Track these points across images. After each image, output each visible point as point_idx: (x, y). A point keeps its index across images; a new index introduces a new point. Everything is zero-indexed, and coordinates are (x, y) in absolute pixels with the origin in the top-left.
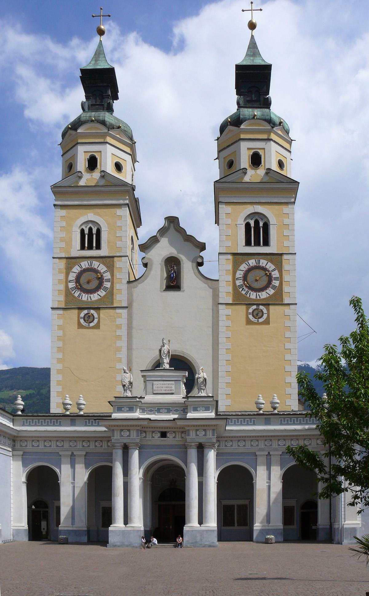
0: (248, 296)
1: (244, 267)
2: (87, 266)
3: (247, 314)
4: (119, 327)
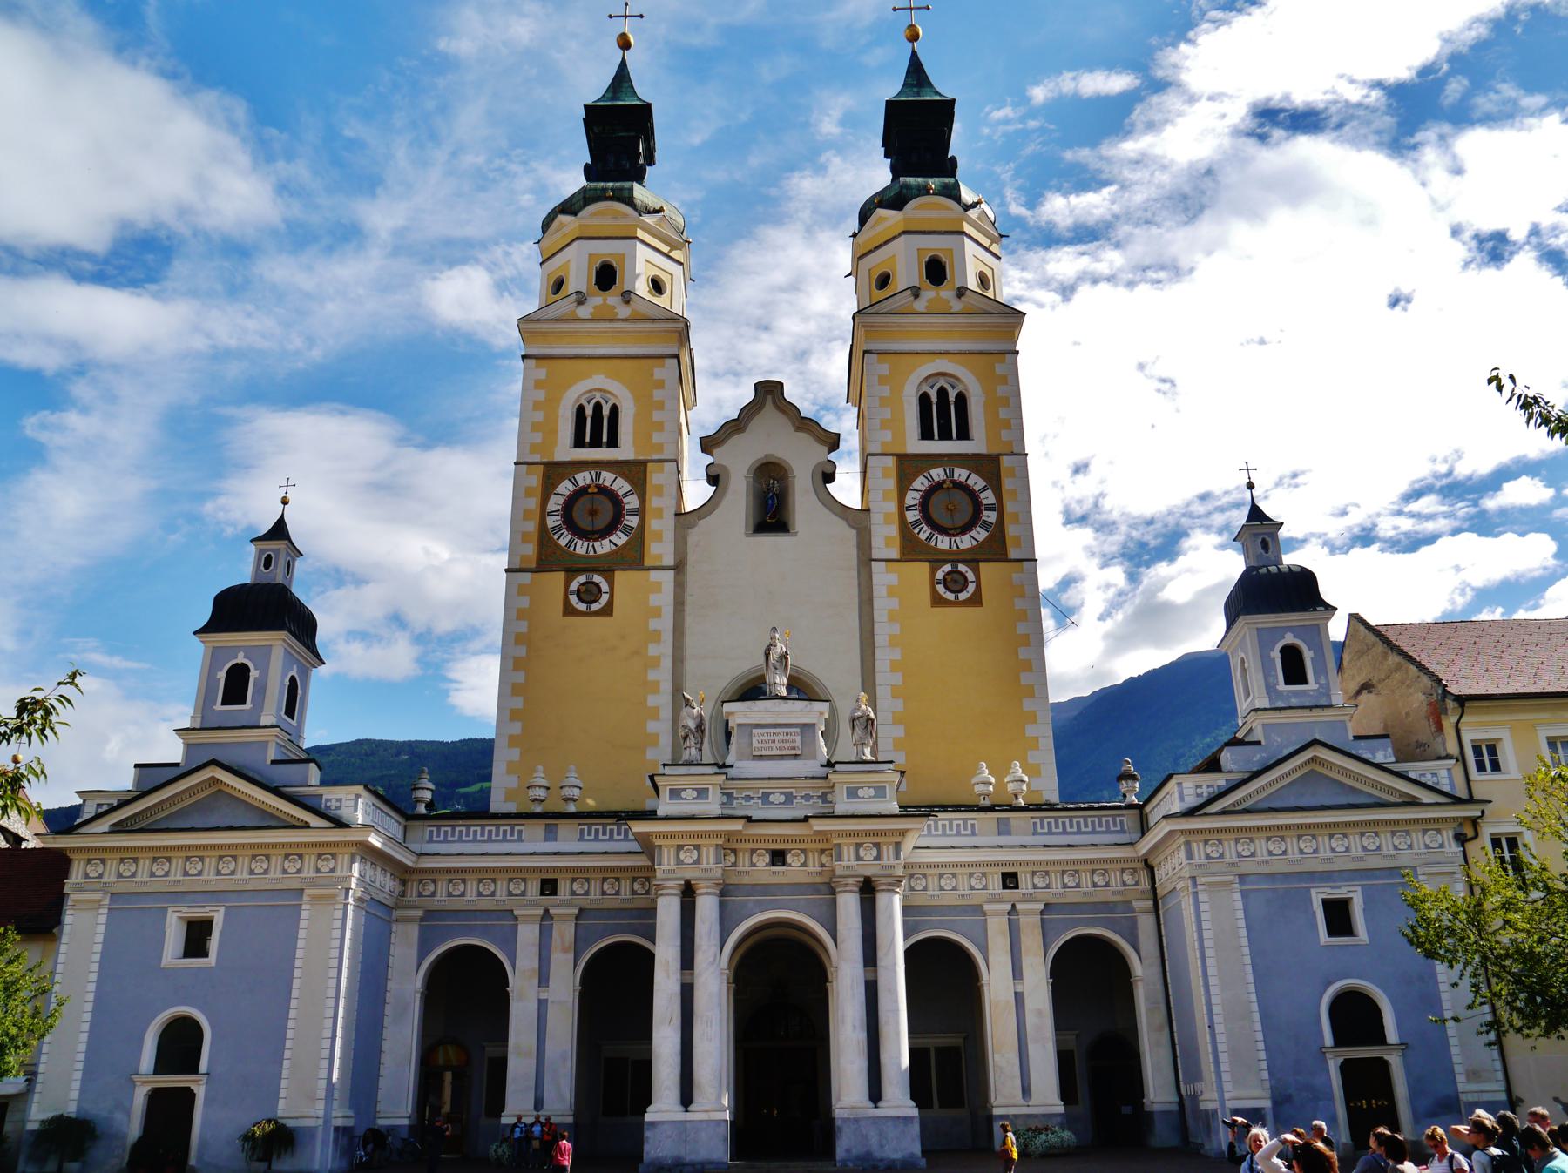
1: (921, 483)
3: (933, 582)
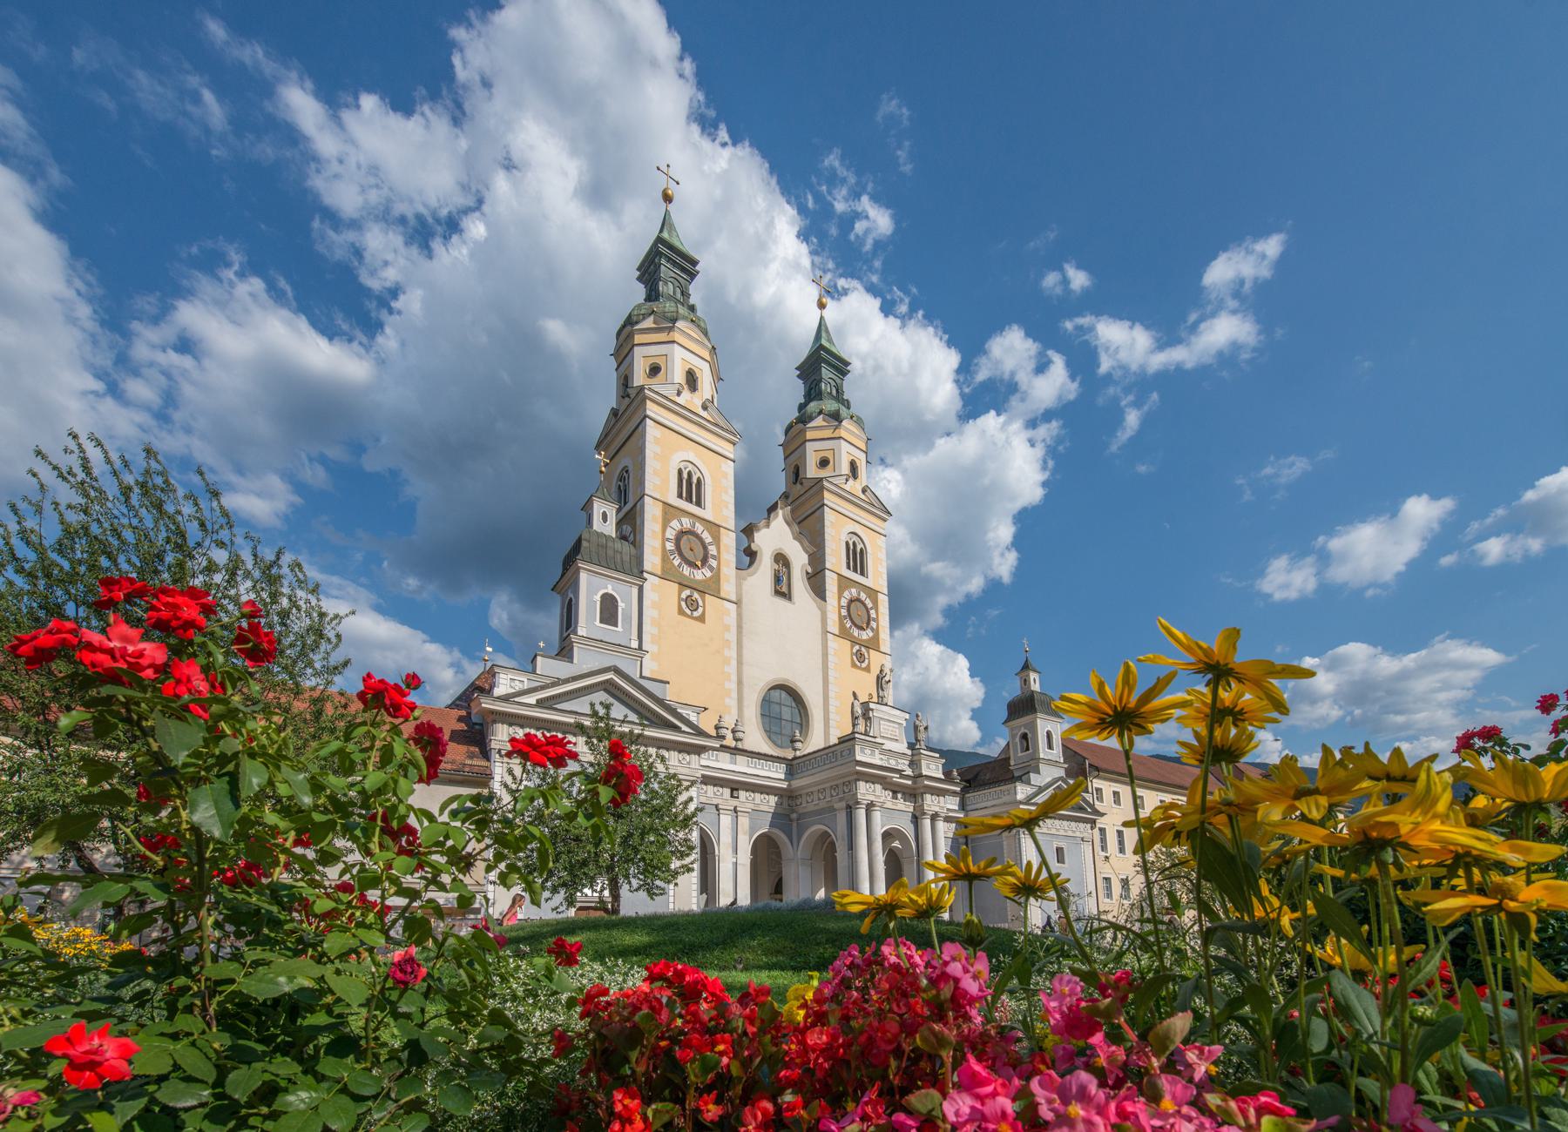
4: (727, 628)
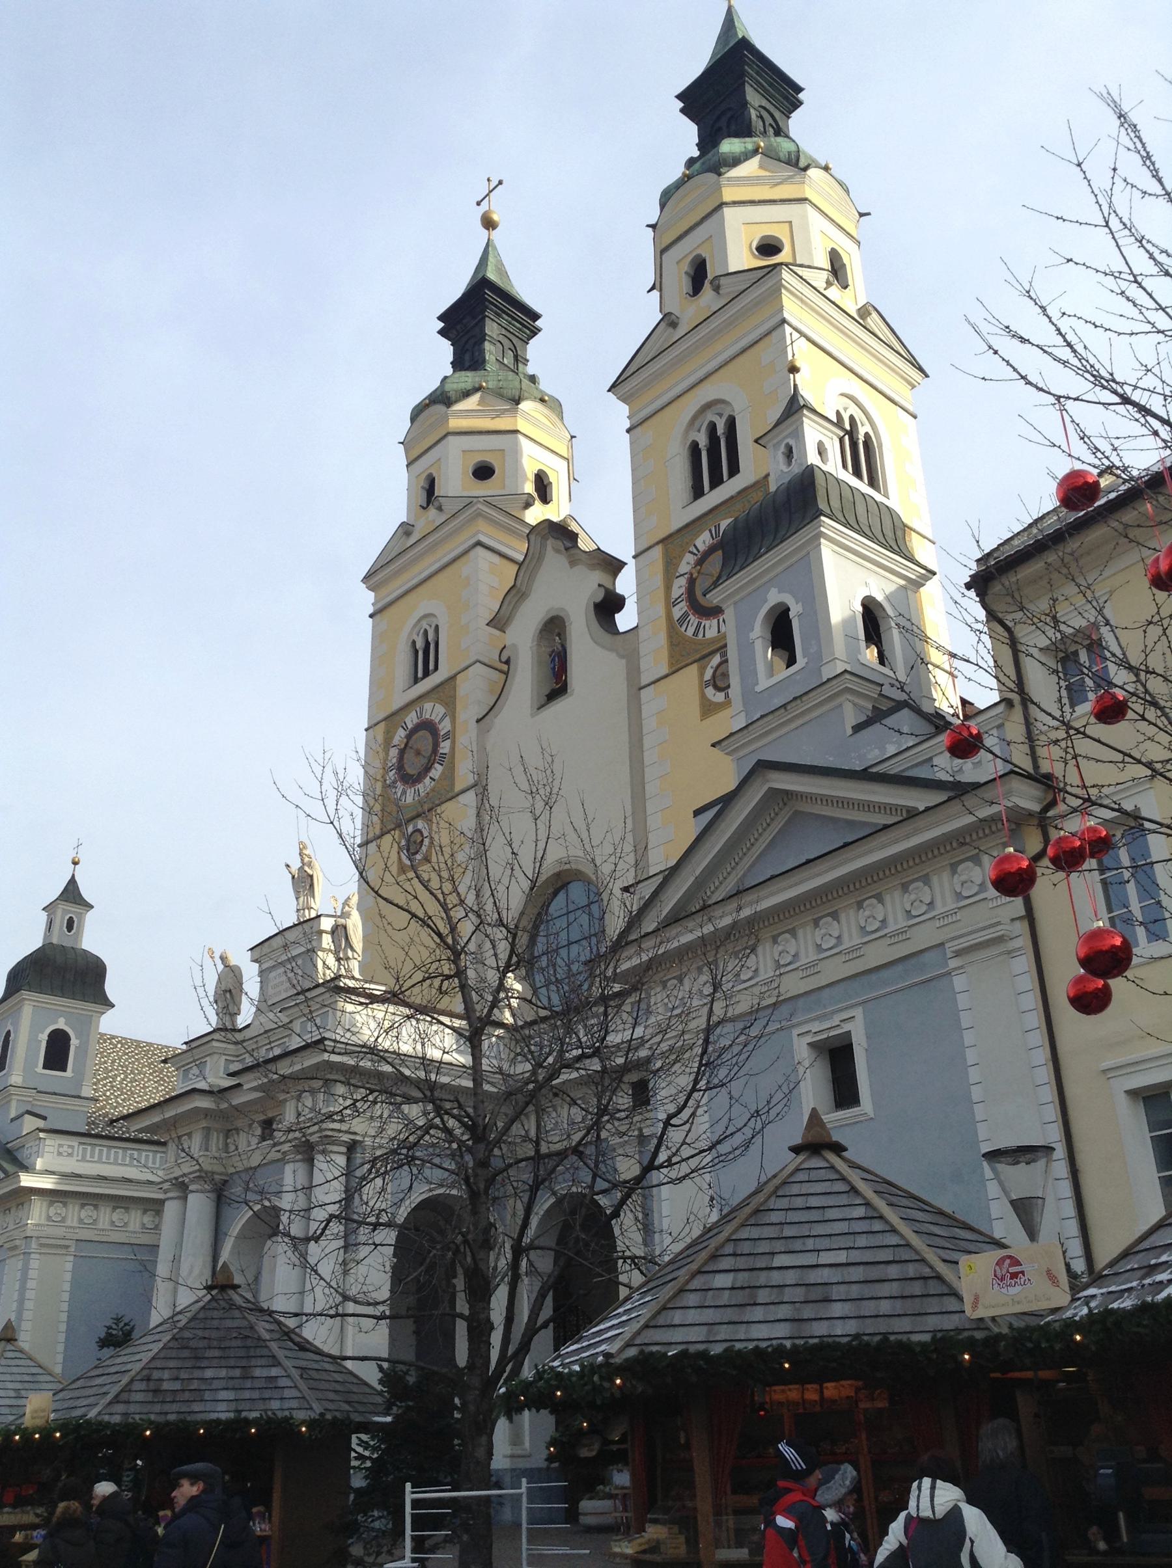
0: (700, 635)
2: (416, 721)
